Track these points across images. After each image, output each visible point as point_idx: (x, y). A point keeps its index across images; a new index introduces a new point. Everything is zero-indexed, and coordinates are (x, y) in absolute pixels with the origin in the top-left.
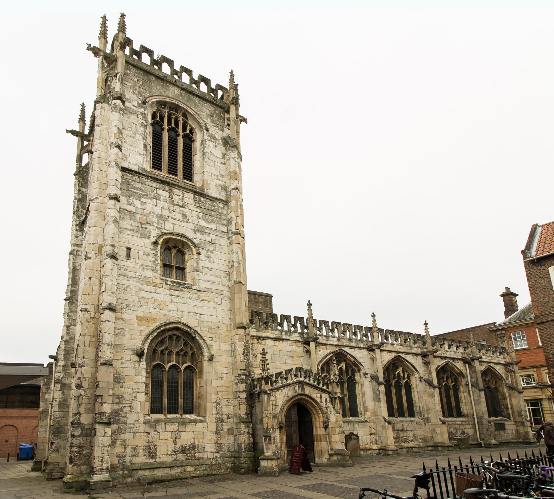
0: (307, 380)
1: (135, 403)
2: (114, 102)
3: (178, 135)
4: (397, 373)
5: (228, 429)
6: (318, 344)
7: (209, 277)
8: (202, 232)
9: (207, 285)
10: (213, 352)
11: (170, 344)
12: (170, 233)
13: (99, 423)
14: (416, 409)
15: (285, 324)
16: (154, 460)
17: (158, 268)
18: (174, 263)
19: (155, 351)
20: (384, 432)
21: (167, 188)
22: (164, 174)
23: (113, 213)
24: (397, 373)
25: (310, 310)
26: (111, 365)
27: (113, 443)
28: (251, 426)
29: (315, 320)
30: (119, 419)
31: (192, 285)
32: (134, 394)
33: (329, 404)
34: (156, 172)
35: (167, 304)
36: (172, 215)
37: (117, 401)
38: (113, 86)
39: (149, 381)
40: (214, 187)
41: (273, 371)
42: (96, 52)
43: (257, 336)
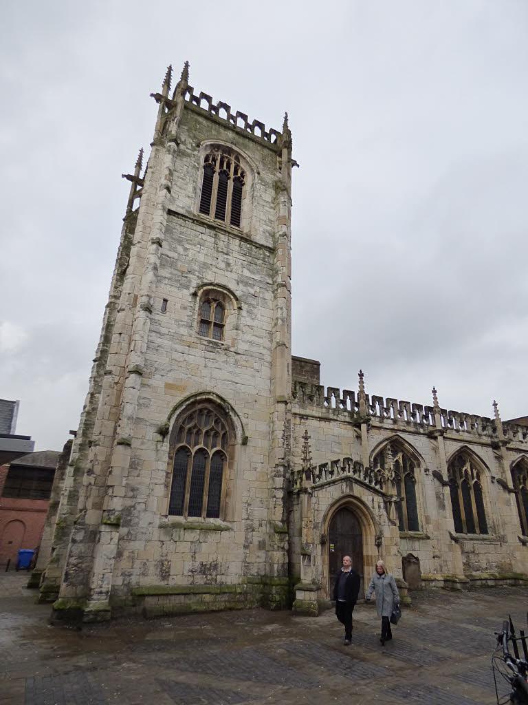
0: (356, 476)
1: (151, 498)
2: (170, 144)
3: (229, 178)
4: (464, 469)
5: (260, 542)
6: (370, 427)
7: (249, 337)
8: (246, 284)
10: (247, 434)
11: (200, 422)
12: (211, 284)
13: (106, 524)
14: (489, 522)
15: (333, 399)
16: (166, 582)
17: (195, 324)
18: (212, 319)
19: (181, 428)
20: (450, 554)
21: (213, 232)
22: (211, 218)
23: (153, 259)
24: (464, 469)
25: (361, 382)
26: (129, 445)
27: (119, 555)
28: (287, 538)
29: (367, 396)
30: (131, 520)
31: (229, 347)
32: (151, 486)
33: (383, 512)
34: (203, 216)
35: (200, 369)
36: (214, 263)
37: (131, 494)
38: (170, 130)
39: (171, 470)
40: (261, 233)
41: (316, 462)
42: (158, 98)
43: (300, 415)
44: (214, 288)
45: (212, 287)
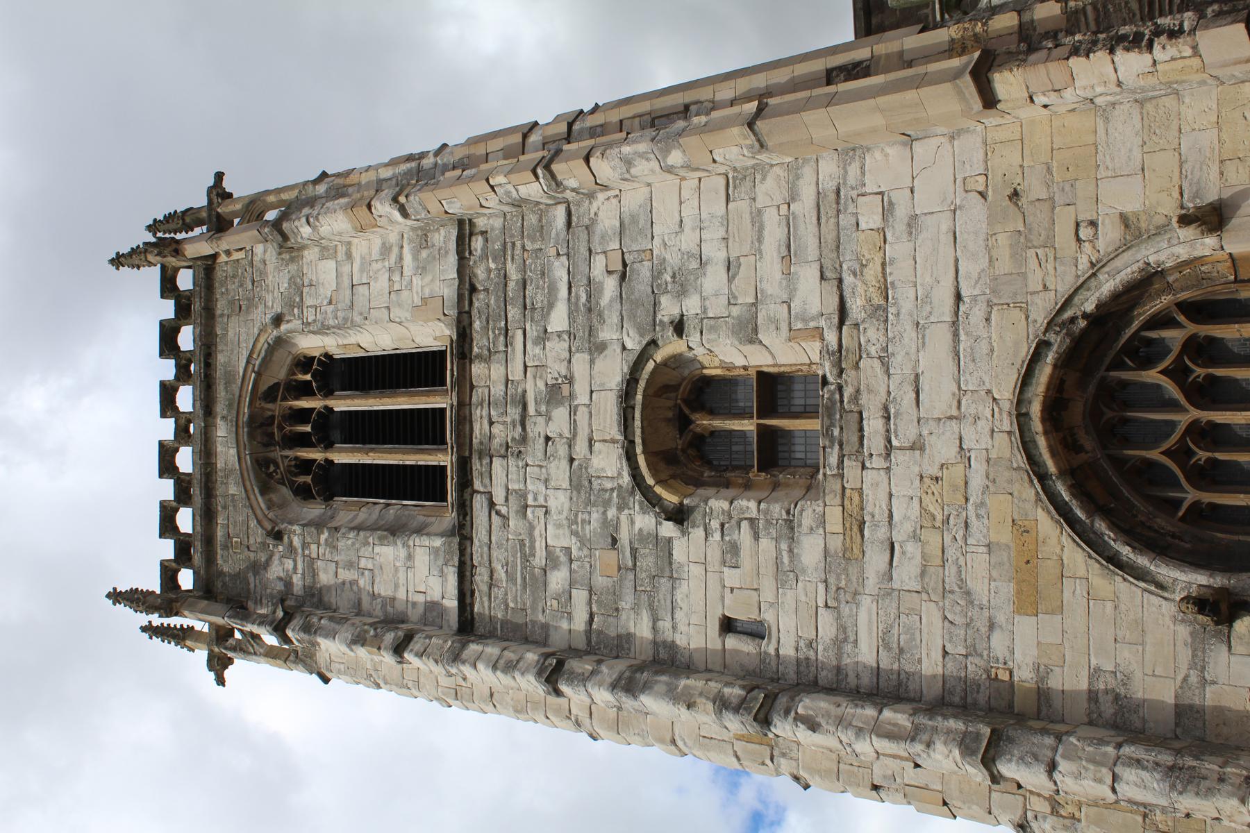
7: (771, 267)
9: (808, 277)
35: (935, 471)
36: (562, 451)
44: (638, 440)
45: (639, 449)
